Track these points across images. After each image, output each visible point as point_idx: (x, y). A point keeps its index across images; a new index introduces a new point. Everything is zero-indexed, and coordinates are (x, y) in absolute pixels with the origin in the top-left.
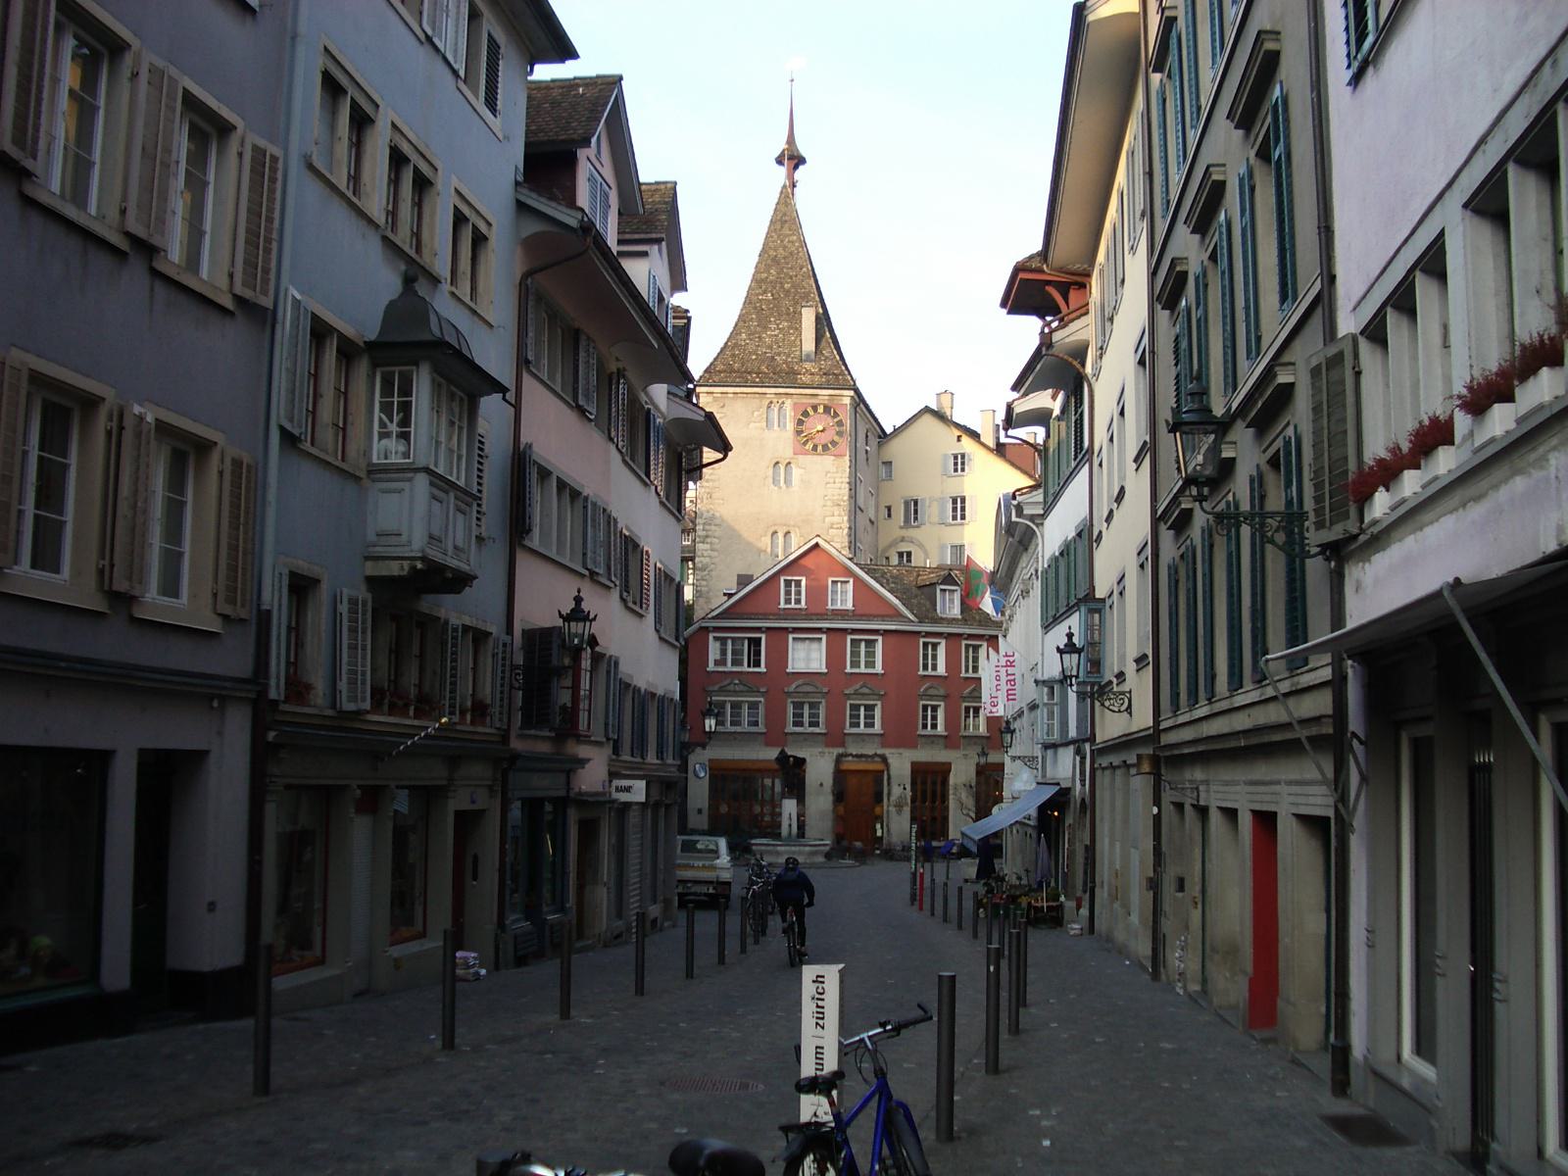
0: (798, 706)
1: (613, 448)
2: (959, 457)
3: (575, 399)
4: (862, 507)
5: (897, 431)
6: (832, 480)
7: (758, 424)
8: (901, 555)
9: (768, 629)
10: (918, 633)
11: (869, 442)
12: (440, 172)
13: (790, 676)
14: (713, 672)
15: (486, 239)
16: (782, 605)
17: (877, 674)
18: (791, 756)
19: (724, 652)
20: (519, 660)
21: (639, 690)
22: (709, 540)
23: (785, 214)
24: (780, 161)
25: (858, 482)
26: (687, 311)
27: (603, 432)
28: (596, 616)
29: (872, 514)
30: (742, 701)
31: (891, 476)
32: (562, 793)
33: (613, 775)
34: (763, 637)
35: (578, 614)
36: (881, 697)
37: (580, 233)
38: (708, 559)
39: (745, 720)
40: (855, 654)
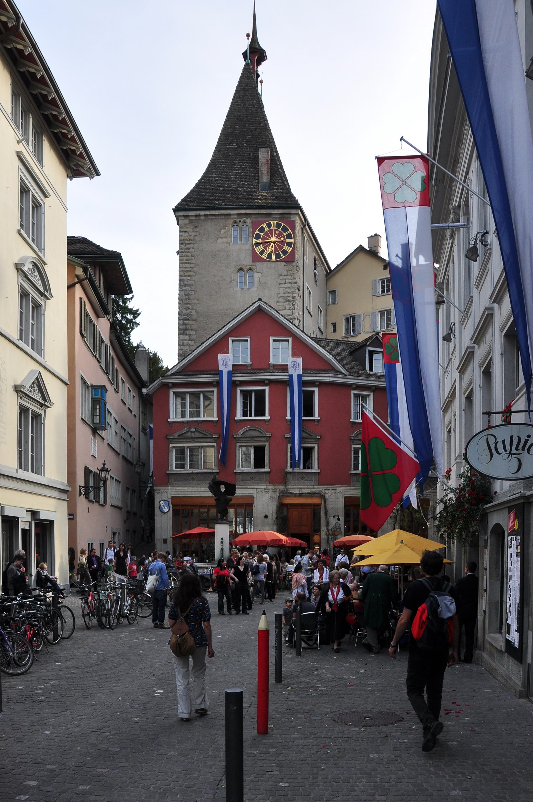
5: (340, 266)
6: (284, 281)
7: (224, 240)
10: (349, 386)
13: (239, 424)
14: (174, 422)
22: (187, 332)
23: (247, 85)
30: (199, 447)
31: (335, 300)
36: (317, 441)
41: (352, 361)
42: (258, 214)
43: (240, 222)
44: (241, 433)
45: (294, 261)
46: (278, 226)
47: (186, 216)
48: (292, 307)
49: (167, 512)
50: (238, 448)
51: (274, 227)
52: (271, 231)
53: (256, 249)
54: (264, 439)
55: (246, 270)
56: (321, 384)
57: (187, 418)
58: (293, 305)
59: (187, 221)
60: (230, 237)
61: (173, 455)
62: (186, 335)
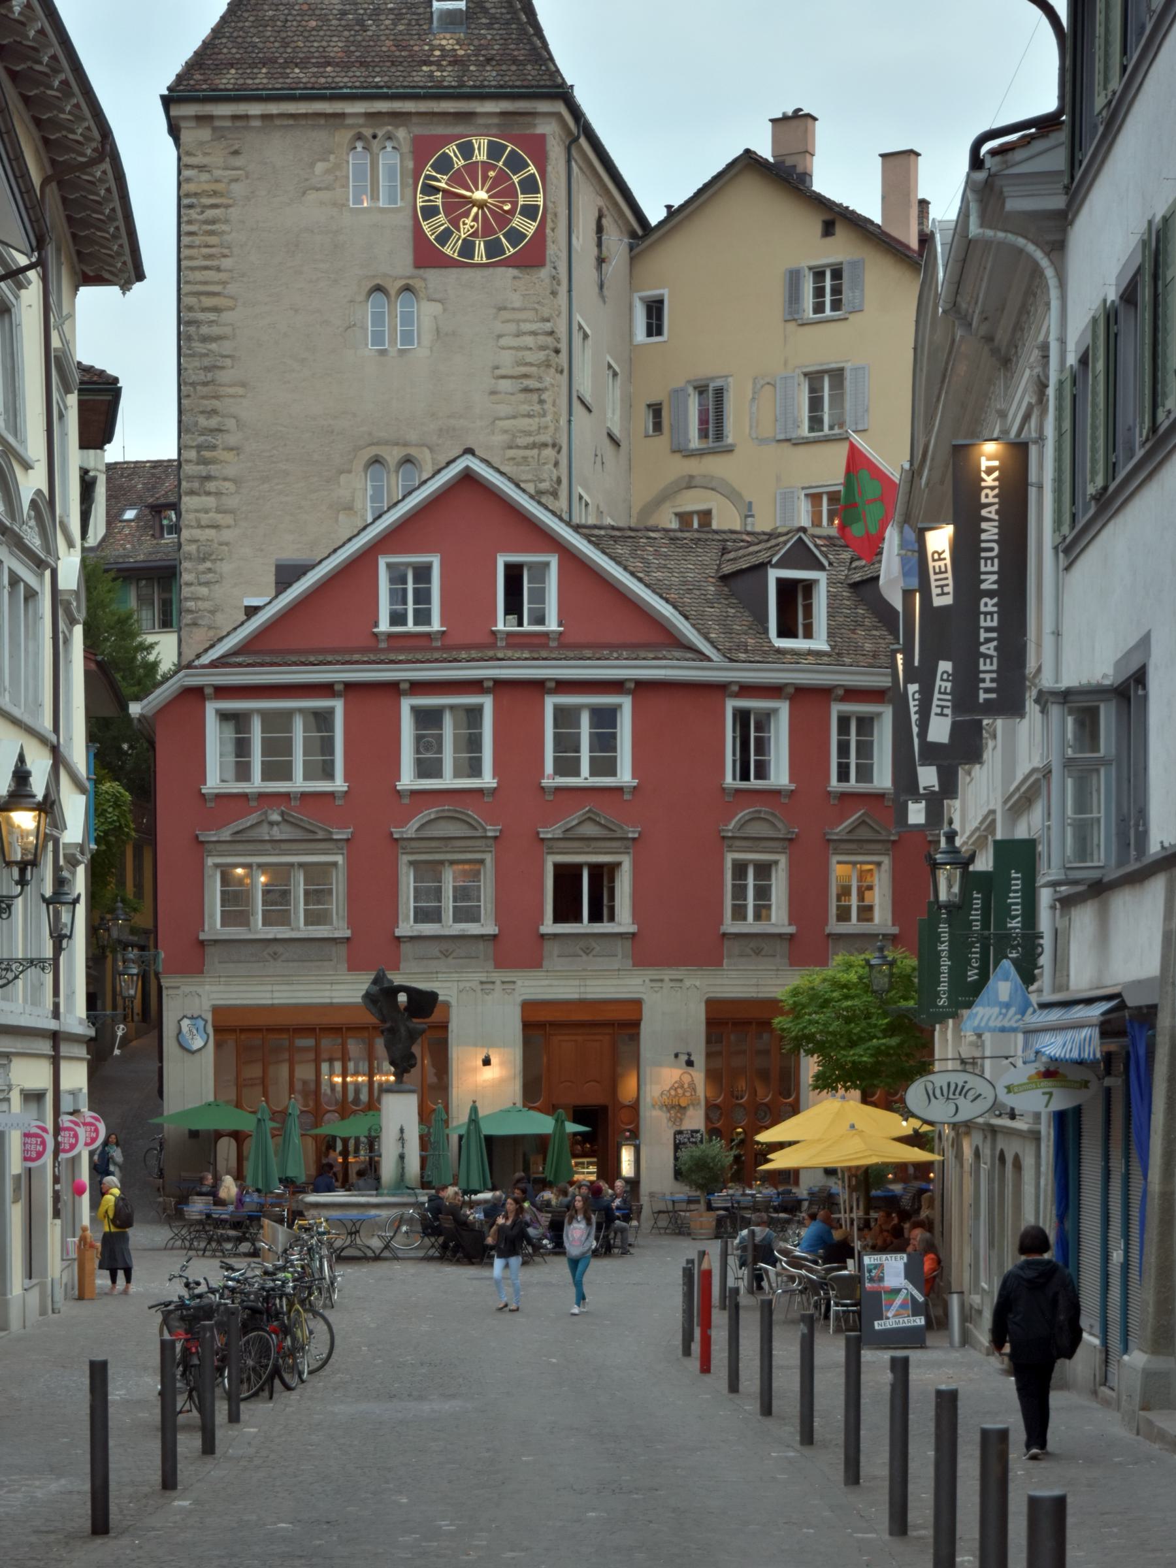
0: (429, 871)
4: (588, 399)
6: (512, 327)
8: (684, 518)
9: (350, 686)
16: (384, 626)
17: (619, 790)
19: (242, 747)
25: (577, 337)
29: (615, 424)
30: (292, 865)
34: (338, 705)
39: (299, 906)
40: (567, 743)
41: (728, 605)
42: (434, 114)
43: (375, 137)
44: (416, 826)
46: (495, 151)
48: (537, 407)
49: (200, 1050)
51: (481, 156)
52: (471, 168)
53: (425, 226)
54: (478, 843)
55: (393, 292)
56: (641, 688)
57: (257, 783)
60: (343, 186)
61: (214, 890)
62: (208, 494)
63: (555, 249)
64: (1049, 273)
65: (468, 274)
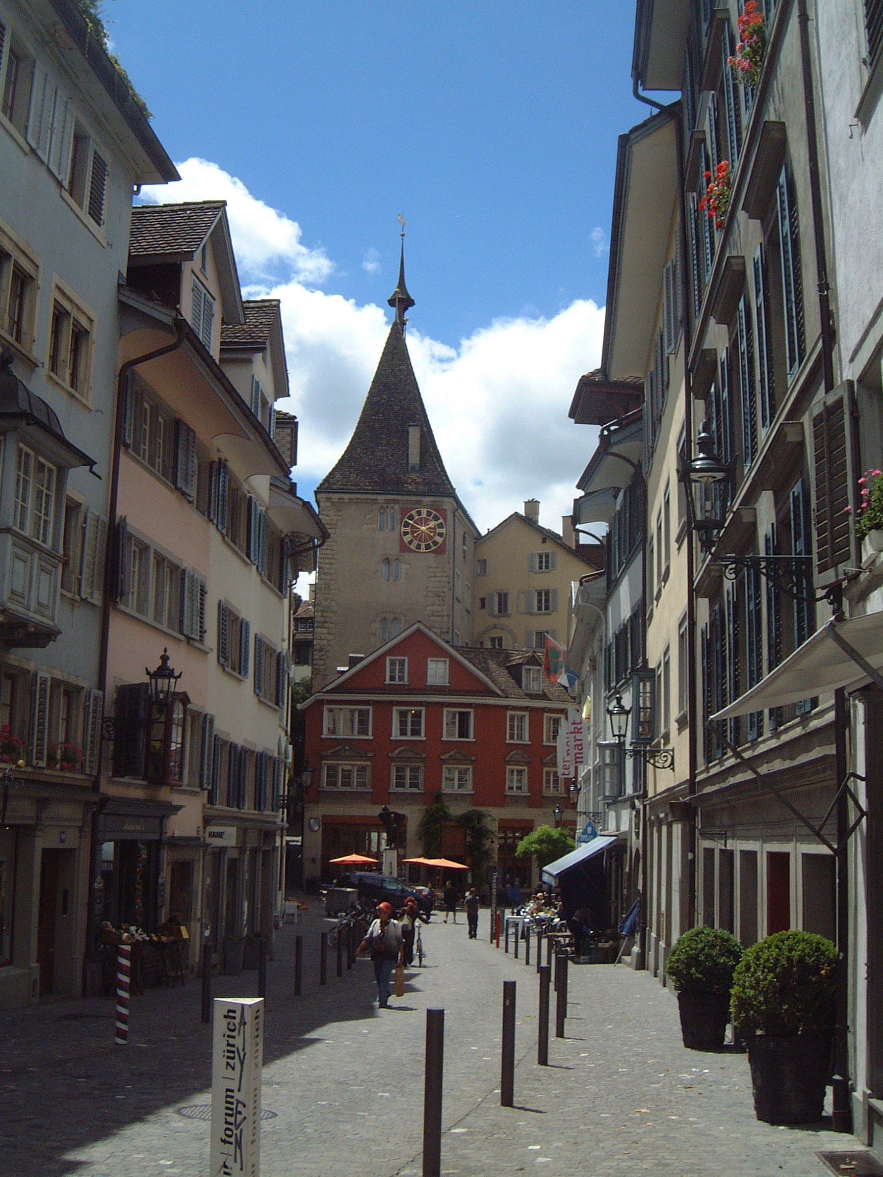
1: (212, 529)
2: (544, 557)
3: (175, 482)
8: (493, 640)
11: (466, 543)
12: (41, 270)
15: (87, 332)
16: (388, 681)
18: (393, 813)
20: (110, 712)
21: (236, 746)
22: (326, 625)
24: (391, 302)
25: (456, 577)
26: (295, 417)
27: (203, 514)
28: (181, 674)
29: (468, 605)
32: (156, 837)
33: (207, 821)
35: (164, 671)
37: (174, 329)
38: (325, 642)
45: (444, 553)
46: (429, 514)
47: (328, 499)
48: (442, 603)
50: (392, 768)
51: (424, 515)
58: (444, 601)
59: (329, 504)
63: (449, 547)
64: (602, 616)
65: (418, 555)
